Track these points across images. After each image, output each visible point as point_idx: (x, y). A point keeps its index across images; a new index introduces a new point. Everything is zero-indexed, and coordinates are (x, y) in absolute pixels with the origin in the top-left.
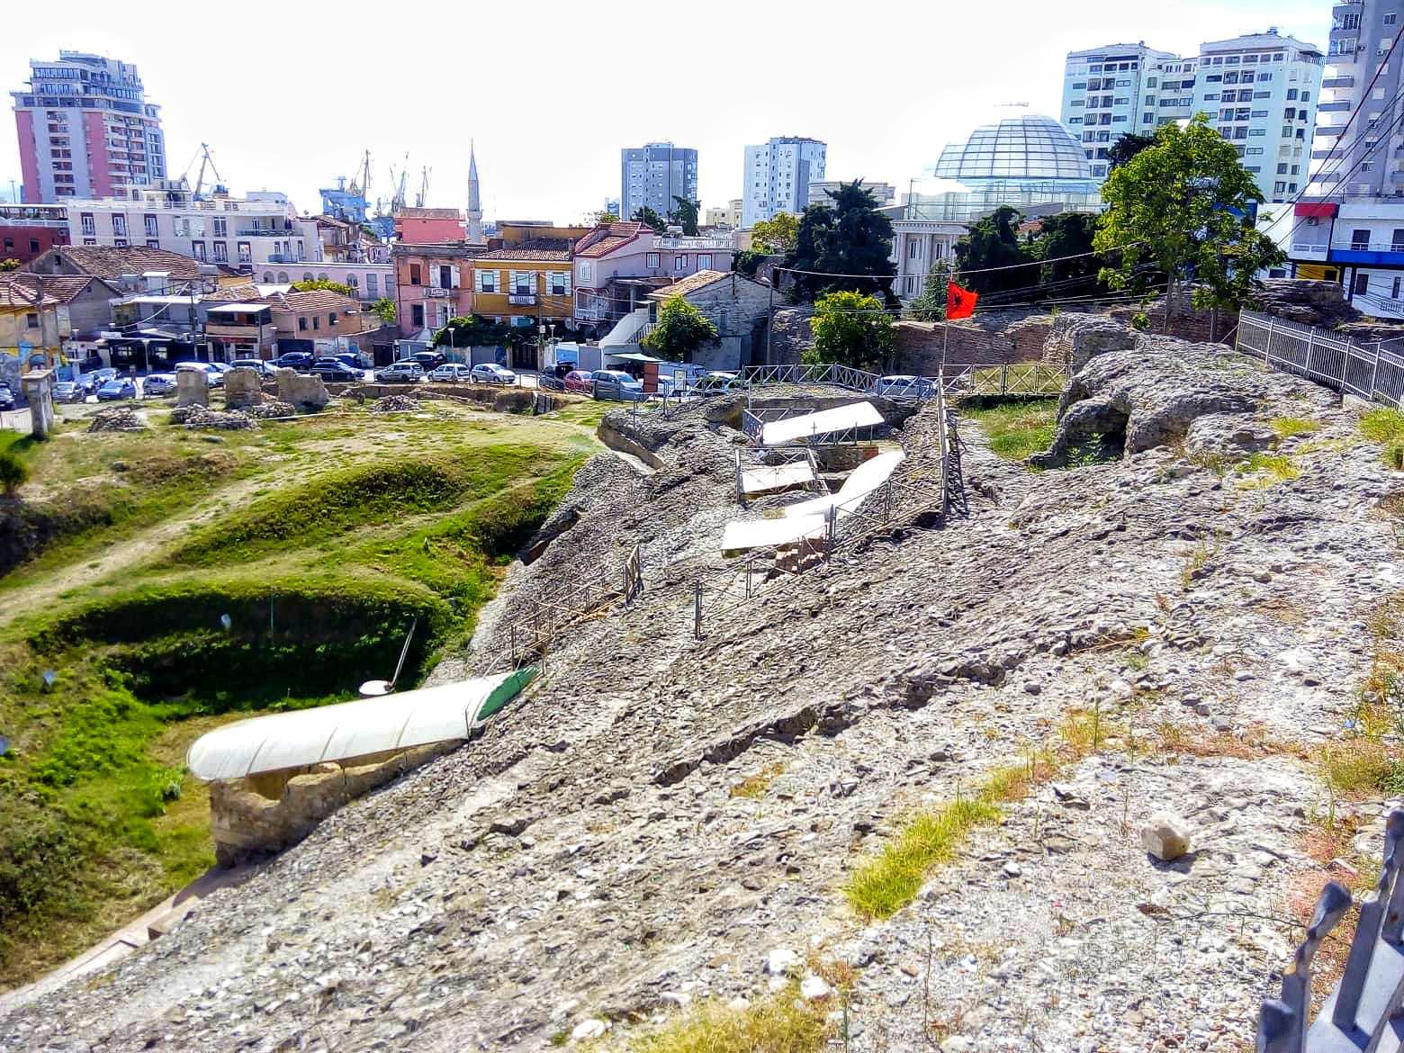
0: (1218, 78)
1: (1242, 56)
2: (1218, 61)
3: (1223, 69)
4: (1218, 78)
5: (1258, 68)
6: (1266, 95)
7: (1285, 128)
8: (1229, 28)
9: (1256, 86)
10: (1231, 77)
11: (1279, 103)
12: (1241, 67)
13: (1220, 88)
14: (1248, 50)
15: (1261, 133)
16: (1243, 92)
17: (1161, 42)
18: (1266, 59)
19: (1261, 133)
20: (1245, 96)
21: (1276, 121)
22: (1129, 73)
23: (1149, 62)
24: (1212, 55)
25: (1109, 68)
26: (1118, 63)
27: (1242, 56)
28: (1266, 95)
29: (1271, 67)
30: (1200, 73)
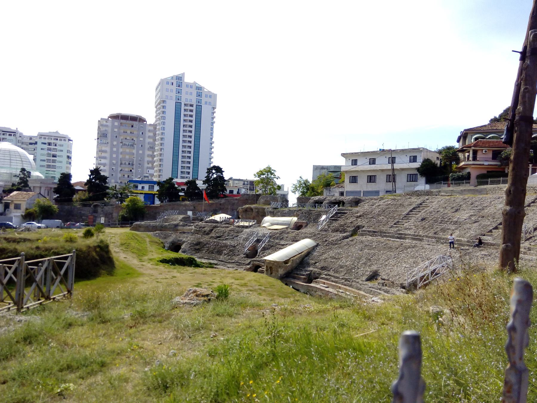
0: (45, 144)
1: (53, 138)
2: (45, 138)
3: (47, 141)
4: (45, 144)
5: (58, 142)
6: (62, 151)
7: (67, 161)
8: (46, 130)
9: (58, 148)
10: (49, 144)
11: (65, 154)
12: (53, 141)
13: (46, 146)
14: (54, 137)
15: (61, 162)
16: (53, 149)
17: (20, 130)
18: (61, 140)
19: (61, 162)
20: (55, 150)
21: (65, 159)
22: (12, 137)
23: (18, 135)
24: (41, 136)
25: (3, 134)
26: (8, 133)
27: (53, 138)
28: (62, 151)
29: (62, 142)
30: (39, 141)
